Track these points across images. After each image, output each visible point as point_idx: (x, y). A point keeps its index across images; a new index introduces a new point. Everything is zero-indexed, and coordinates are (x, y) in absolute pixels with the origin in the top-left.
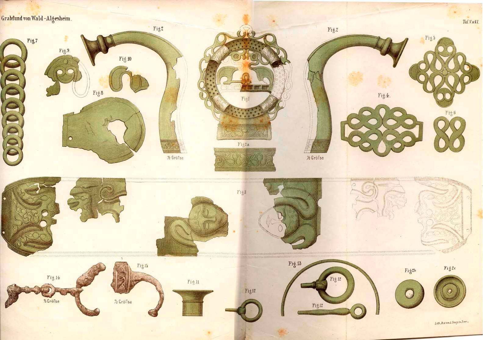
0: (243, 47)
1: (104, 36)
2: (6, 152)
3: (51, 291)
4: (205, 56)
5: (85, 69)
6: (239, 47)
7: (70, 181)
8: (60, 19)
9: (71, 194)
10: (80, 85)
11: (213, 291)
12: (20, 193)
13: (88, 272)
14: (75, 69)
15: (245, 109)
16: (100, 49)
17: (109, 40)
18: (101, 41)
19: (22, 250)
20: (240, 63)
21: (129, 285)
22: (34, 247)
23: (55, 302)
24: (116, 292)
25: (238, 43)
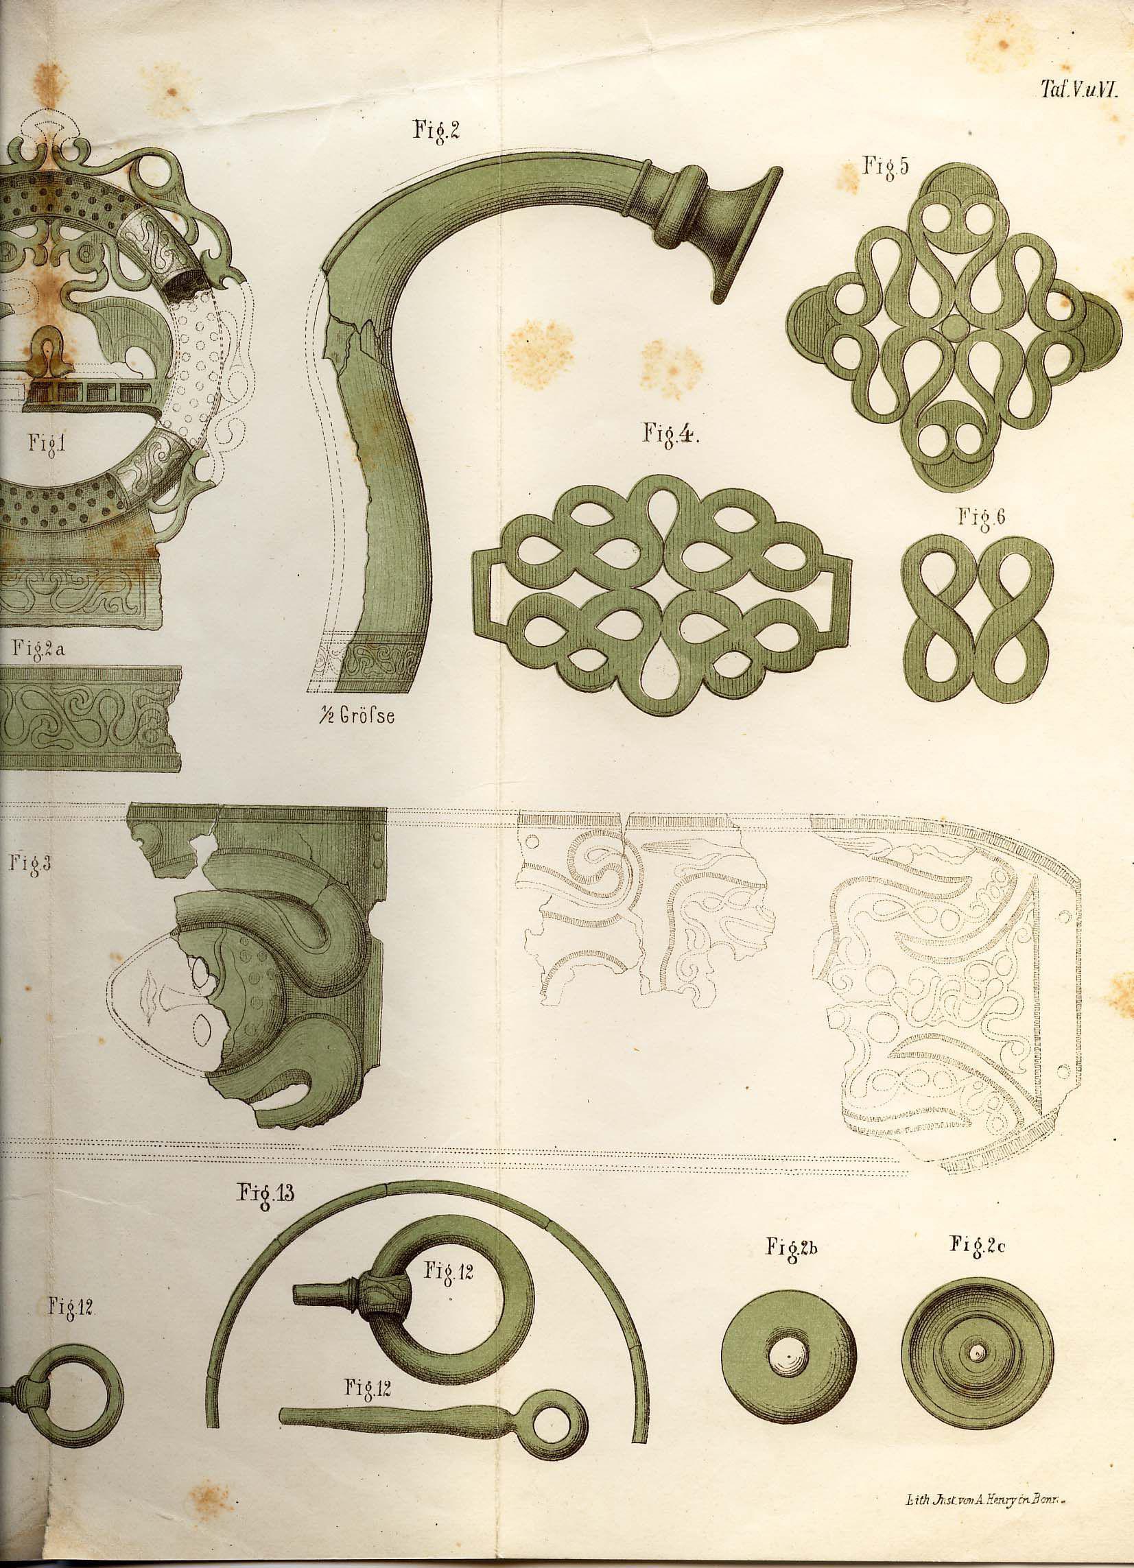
0: (33, 208)
6: (16, 212)
15: (41, 489)
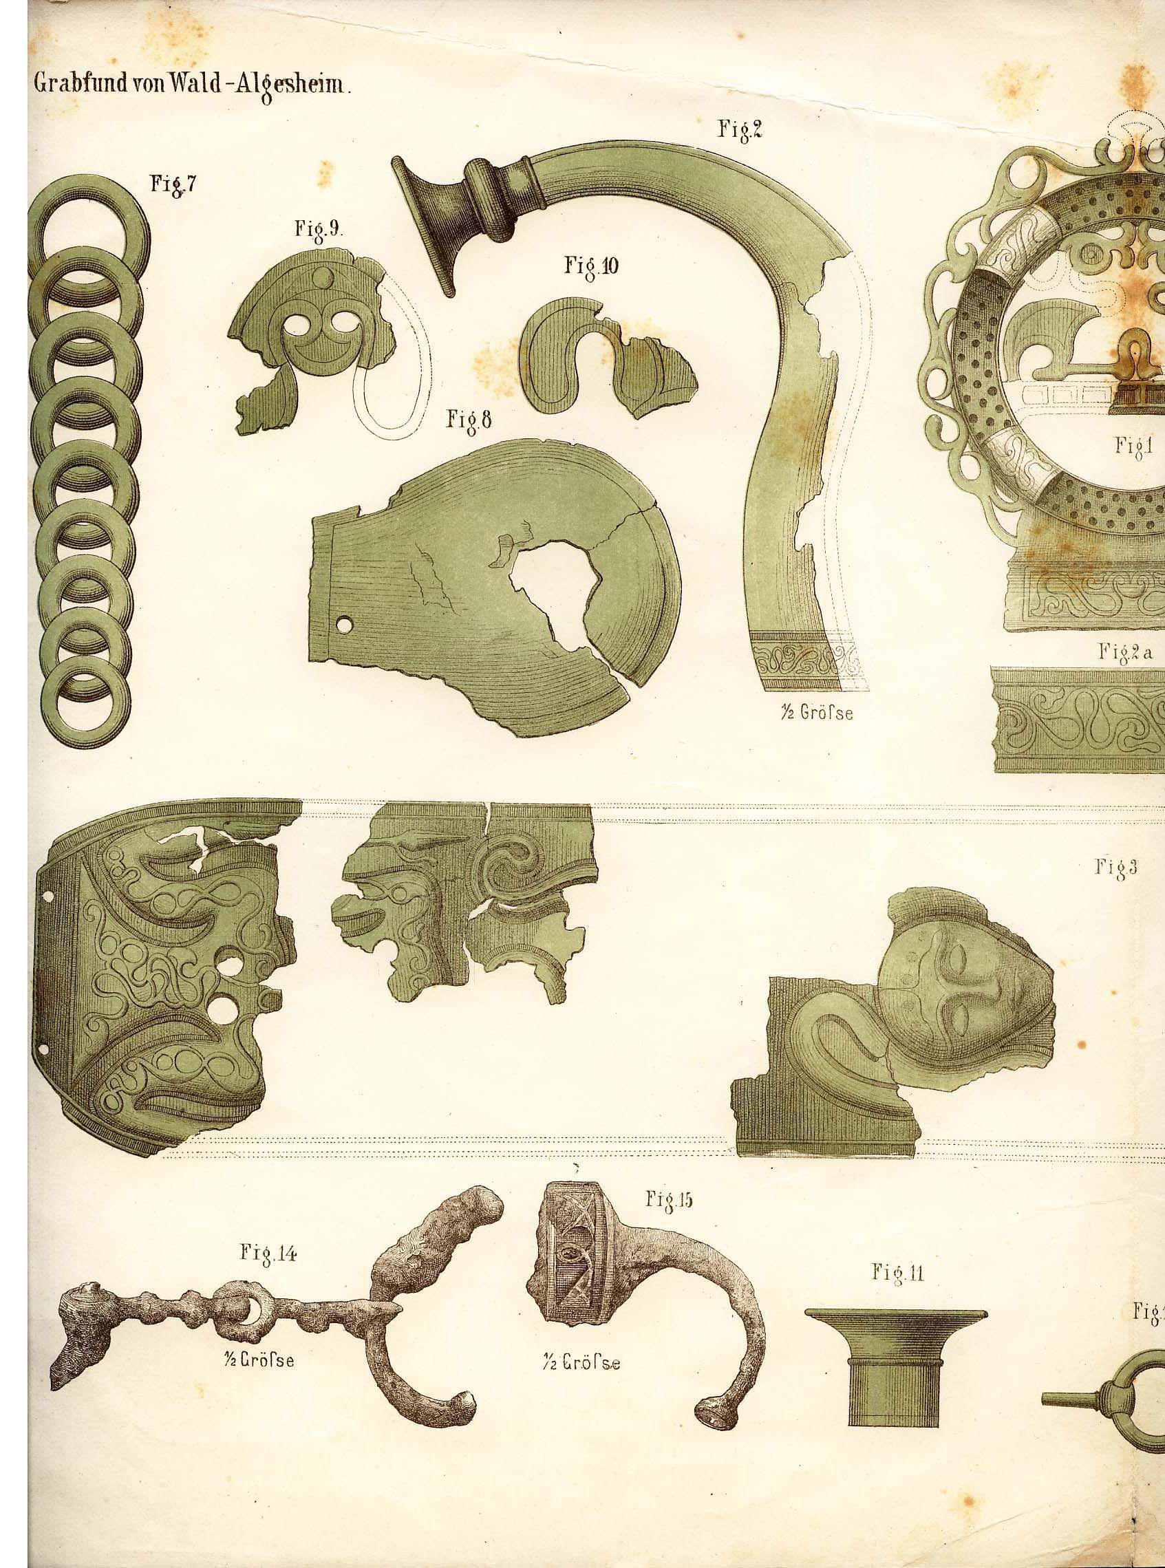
0: (1119, 211)
1: (497, 163)
2: (55, 684)
3: (257, 1315)
4: (951, 253)
5: (410, 312)
6: (1102, 214)
7: (344, 816)
8: (299, 84)
9: (346, 877)
10: (388, 383)
11: (986, 1315)
12: (118, 872)
13: (423, 1230)
14: (366, 313)
15: (1128, 492)
16: (476, 221)
17: (518, 183)
18: (481, 185)
19: (128, 1130)
20: (1108, 286)
21: (608, 1286)
22: (181, 1114)
23: (275, 1362)
24: (548, 1318)
25: (1100, 195)
